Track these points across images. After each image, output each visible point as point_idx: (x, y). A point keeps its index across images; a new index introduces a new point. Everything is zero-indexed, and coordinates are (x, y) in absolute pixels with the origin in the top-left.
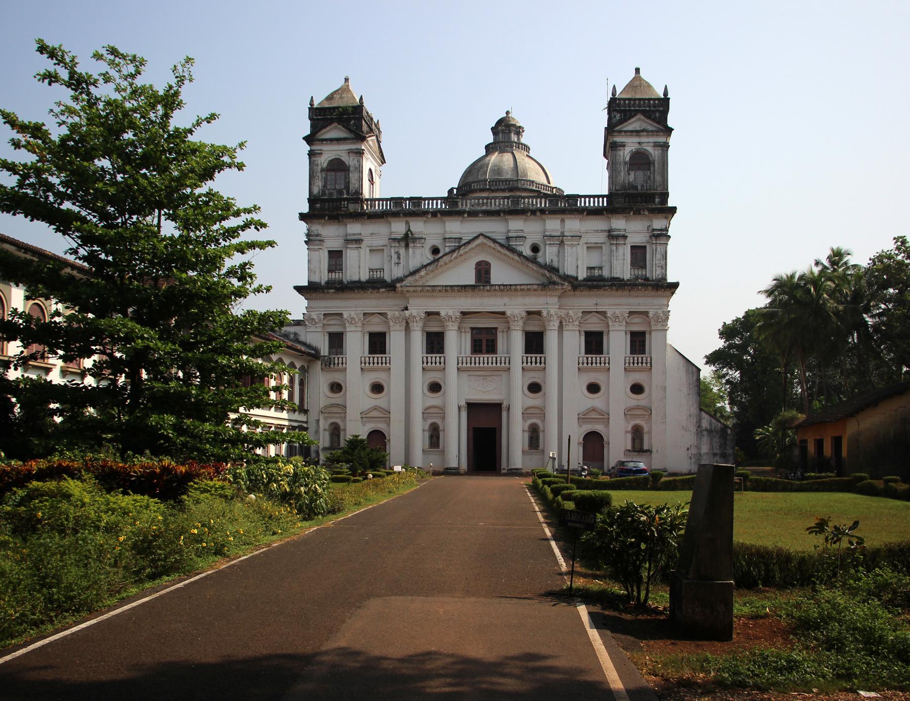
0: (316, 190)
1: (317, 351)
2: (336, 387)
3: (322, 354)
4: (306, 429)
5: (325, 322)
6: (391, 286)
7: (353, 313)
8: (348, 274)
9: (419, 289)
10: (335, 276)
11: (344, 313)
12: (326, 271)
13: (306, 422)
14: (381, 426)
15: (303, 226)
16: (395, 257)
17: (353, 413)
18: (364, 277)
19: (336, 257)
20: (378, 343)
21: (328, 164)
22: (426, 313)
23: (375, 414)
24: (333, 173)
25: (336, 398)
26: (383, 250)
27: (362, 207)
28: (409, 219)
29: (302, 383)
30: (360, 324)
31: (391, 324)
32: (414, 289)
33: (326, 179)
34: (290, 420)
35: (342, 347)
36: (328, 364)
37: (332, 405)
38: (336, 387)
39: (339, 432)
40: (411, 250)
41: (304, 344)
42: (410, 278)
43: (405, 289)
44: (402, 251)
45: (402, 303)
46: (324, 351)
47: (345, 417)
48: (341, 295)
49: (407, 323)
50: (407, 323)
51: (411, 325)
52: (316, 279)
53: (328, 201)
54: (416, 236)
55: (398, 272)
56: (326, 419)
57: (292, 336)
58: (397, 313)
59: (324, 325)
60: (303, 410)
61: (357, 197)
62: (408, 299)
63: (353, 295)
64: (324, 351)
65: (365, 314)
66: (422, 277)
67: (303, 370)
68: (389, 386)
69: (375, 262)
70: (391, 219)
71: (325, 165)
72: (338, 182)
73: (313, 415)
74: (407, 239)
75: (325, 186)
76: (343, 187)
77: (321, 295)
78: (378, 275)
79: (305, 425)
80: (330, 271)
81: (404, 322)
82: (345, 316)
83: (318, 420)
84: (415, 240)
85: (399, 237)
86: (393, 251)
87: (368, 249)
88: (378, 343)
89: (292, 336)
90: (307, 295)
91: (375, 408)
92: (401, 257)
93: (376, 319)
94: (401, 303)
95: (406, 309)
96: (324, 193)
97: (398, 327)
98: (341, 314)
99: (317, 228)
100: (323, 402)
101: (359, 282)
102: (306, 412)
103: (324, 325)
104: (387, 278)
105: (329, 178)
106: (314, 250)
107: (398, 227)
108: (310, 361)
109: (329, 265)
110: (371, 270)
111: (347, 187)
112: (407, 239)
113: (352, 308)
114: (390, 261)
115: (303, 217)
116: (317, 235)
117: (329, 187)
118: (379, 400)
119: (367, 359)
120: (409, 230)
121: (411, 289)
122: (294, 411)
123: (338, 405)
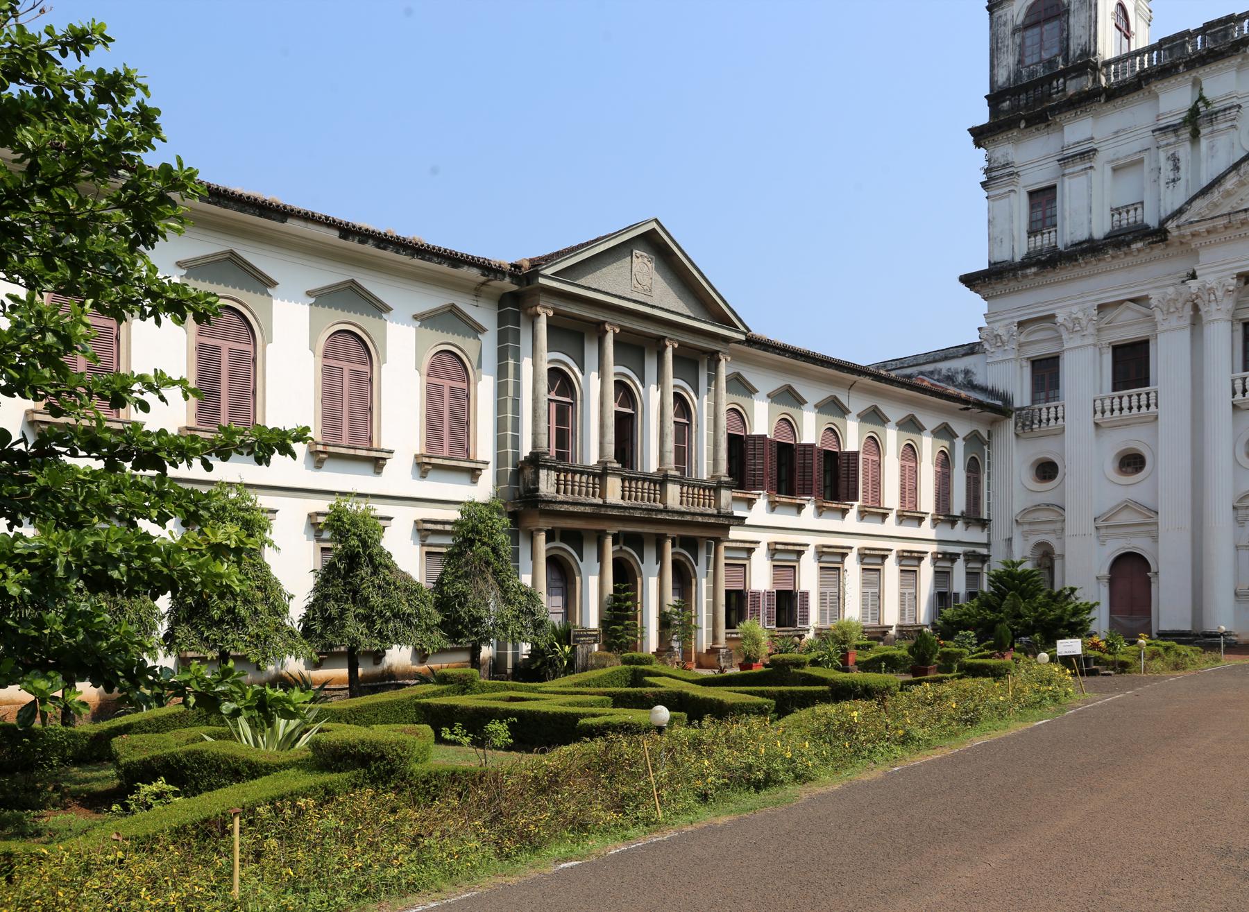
0: (1002, 77)
1: (1006, 399)
2: (1046, 470)
3: (1017, 404)
4: (984, 559)
5: (1022, 339)
6: (1157, 235)
7: (1075, 309)
8: (1067, 230)
9: (1220, 222)
10: (1042, 241)
11: (1057, 312)
12: (1026, 235)
13: (987, 545)
14: (1139, 544)
15: (980, 156)
16: (1166, 167)
17: (1079, 521)
18: (1100, 229)
19: (1043, 199)
20: (1131, 364)
21: (1027, 16)
22: (1239, 276)
23: (1125, 518)
24: (1036, 30)
25: (1046, 492)
26: (1141, 161)
27: (1096, 80)
28: (1200, 72)
29: (973, 468)
30: (1091, 330)
31: (1159, 316)
32: (1209, 225)
33: (1022, 46)
34: (940, 542)
35: (1058, 387)
36: (1028, 423)
37: (1037, 508)
38: (1046, 470)
39: (1052, 561)
40: (1204, 143)
41: (983, 390)
42: (1198, 203)
43: (1187, 231)
44: (1184, 151)
45: (1183, 266)
46: (1022, 396)
47: (1063, 530)
48: (1051, 276)
49: (1196, 308)
50: (1196, 308)
51: (1203, 309)
52: (1004, 255)
53: (1025, 88)
54: (1218, 106)
55: (1173, 199)
56: (1025, 536)
57: (960, 378)
58: (1171, 290)
59: (1020, 345)
60: (974, 518)
61: (1086, 63)
62: (1195, 253)
63: (1077, 271)
64: (1022, 396)
65: (1101, 308)
66: (1228, 194)
67: (974, 440)
68: (1155, 456)
69: (1125, 191)
70: (1157, 87)
71: (1019, 21)
72: (1047, 44)
73: (1000, 529)
74: (1195, 121)
75: (1020, 62)
76: (1056, 51)
77: (1013, 284)
78: (1128, 219)
79: (984, 551)
80: (1032, 233)
81: (1189, 306)
82: (1060, 319)
83: (1010, 540)
84: (1212, 117)
85: (1176, 120)
86: (1162, 155)
87: (1108, 168)
88: (1131, 364)
89: (960, 378)
90: (988, 291)
91: (1126, 506)
92: (1182, 165)
93: (1128, 314)
94: (1181, 266)
95: (1193, 276)
96: (1018, 74)
97: (1174, 322)
98: (1053, 316)
99: (1006, 150)
100: (1019, 502)
101: (1090, 240)
102: (984, 524)
103: (1020, 345)
104: (1152, 221)
105: (1028, 42)
106: (1000, 197)
107: (1175, 99)
108: (993, 422)
109: (1031, 222)
110: (1117, 211)
111: (1065, 51)
112: (1195, 121)
113: (1071, 298)
114: (1157, 181)
115: (980, 135)
116: (1005, 166)
117: (1028, 61)
118: (1136, 487)
119: (1107, 403)
120: (1202, 98)
121: (1202, 228)
122: (952, 521)
123: (1048, 506)
